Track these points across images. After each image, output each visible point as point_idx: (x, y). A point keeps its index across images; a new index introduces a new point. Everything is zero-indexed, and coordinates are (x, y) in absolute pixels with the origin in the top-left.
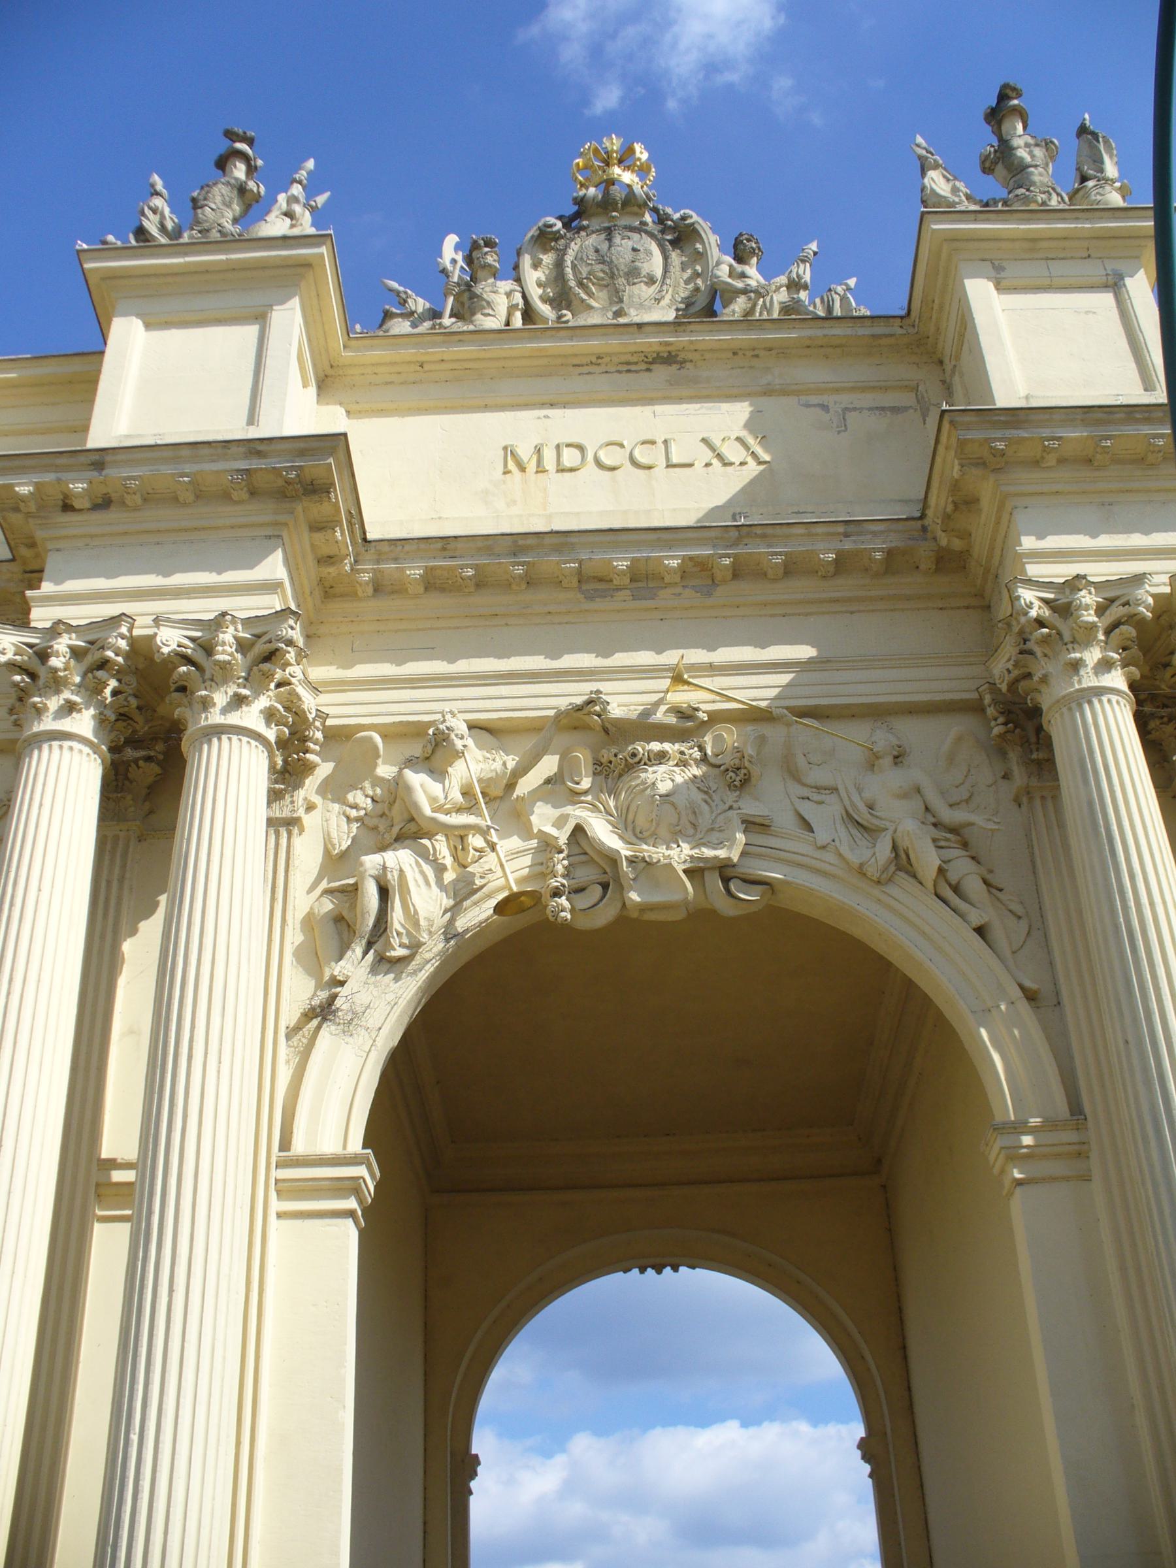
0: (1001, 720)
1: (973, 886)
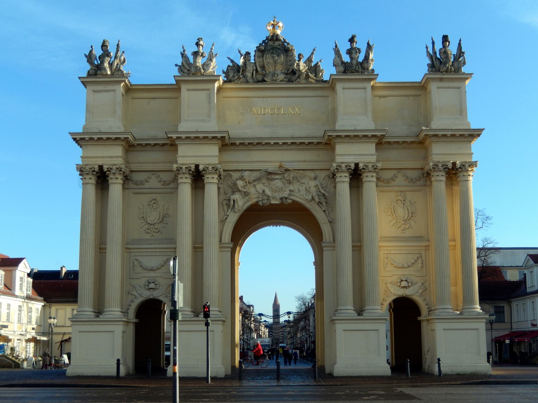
1: (324, 204)
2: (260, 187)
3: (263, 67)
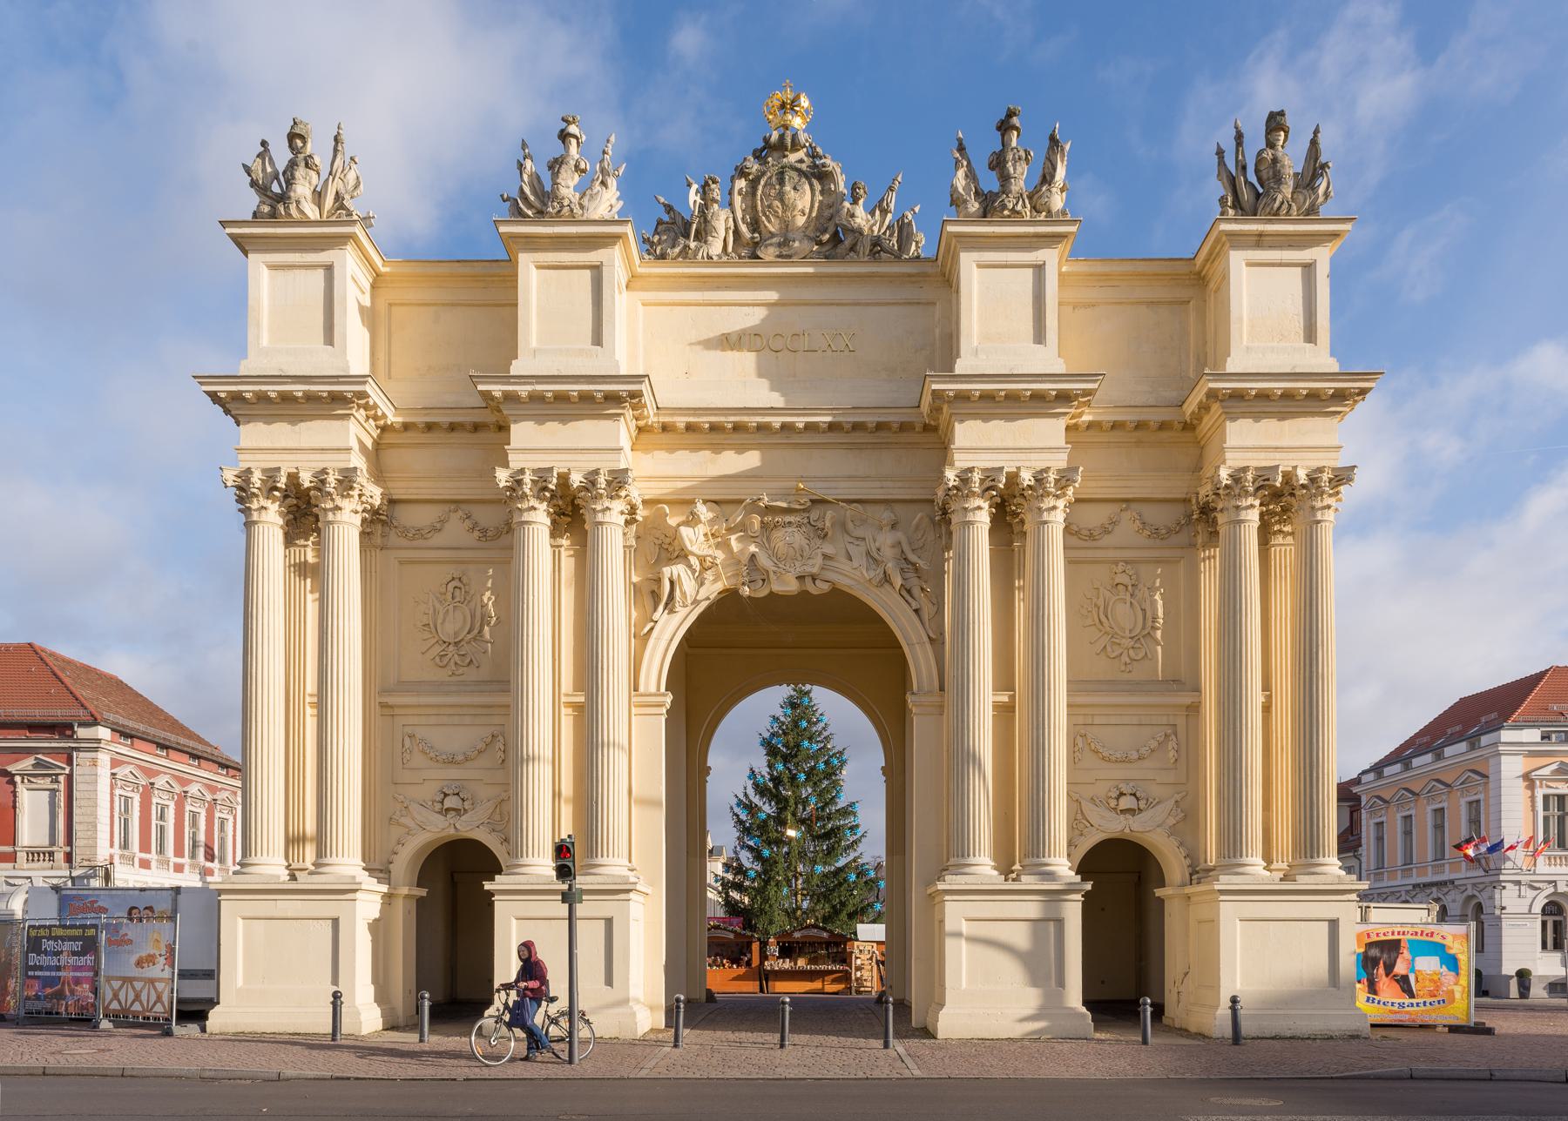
0: (940, 513)
1: (916, 591)
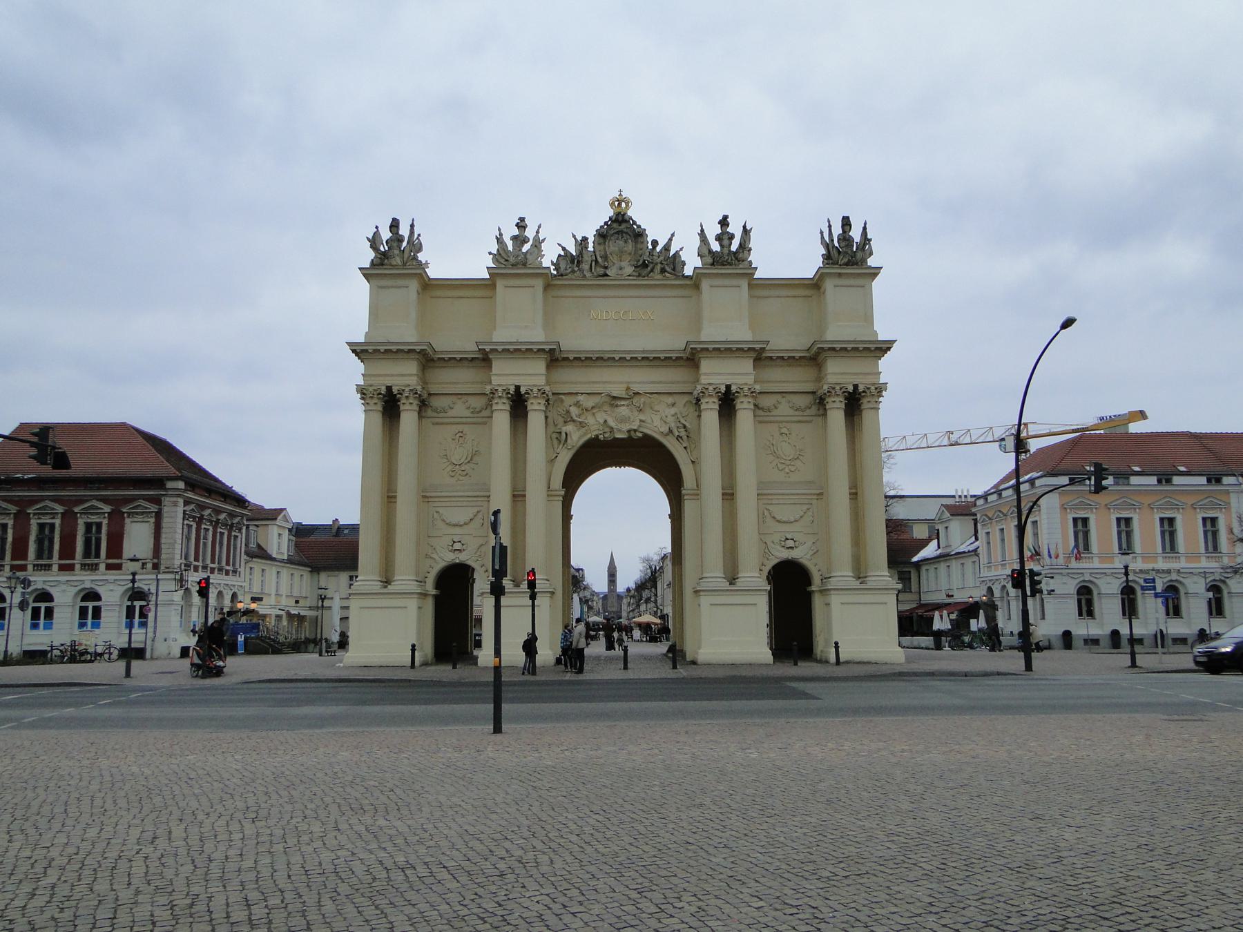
2: (601, 417)
3: (605, 257)
